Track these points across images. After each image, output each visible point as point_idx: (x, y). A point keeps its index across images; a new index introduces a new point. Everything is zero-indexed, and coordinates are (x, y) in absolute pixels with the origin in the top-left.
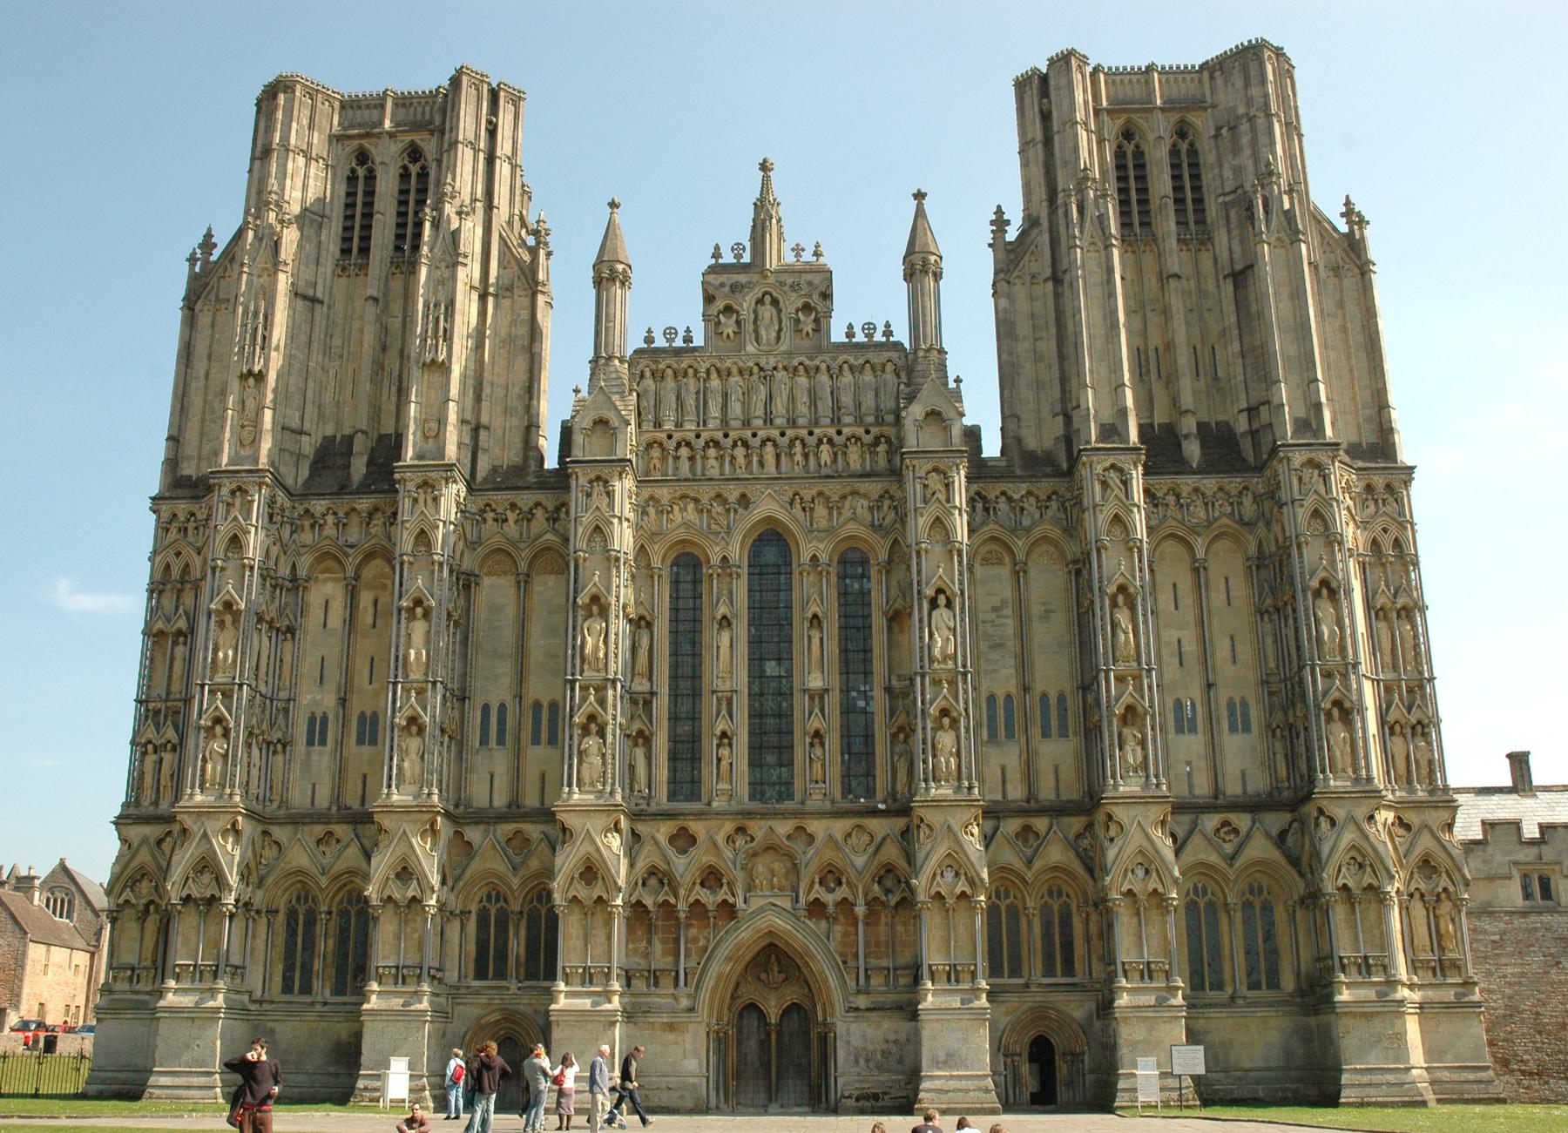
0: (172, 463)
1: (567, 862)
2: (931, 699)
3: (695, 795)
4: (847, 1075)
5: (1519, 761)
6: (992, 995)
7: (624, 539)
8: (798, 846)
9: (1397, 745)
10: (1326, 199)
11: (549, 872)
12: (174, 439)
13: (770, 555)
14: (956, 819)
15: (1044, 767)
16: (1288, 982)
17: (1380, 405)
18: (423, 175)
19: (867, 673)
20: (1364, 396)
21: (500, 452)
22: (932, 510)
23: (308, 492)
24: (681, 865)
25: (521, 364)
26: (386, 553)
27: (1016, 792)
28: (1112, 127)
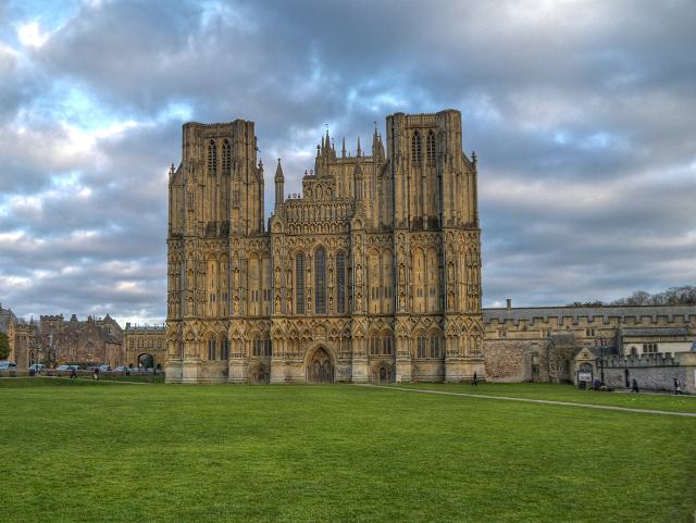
0: (170, 231)
1: (272, 329)
2: (356, 290)
3: (302, 313)
4: (338, 376)
5: (509, 301)
6: (369, 358)
7: (284, 253)
8: (327, 324)
9: (471, 300)
10: (467, 152)
11: (269, 331)
12: (170, 224)
13: (320, 253)
14: (361, 319)
15: (385, 305)
16: (440, 356)
17: (475, 212)
18: (229, 147)
19: (343, 283)
20: (471, 209)
21: (253, 226)
22: (358, 245)
23: (206, 238)
24: (300, 329)
25: (257, 202)
26: (227, 254)
27: (378, 311)
28: (411, 132)
